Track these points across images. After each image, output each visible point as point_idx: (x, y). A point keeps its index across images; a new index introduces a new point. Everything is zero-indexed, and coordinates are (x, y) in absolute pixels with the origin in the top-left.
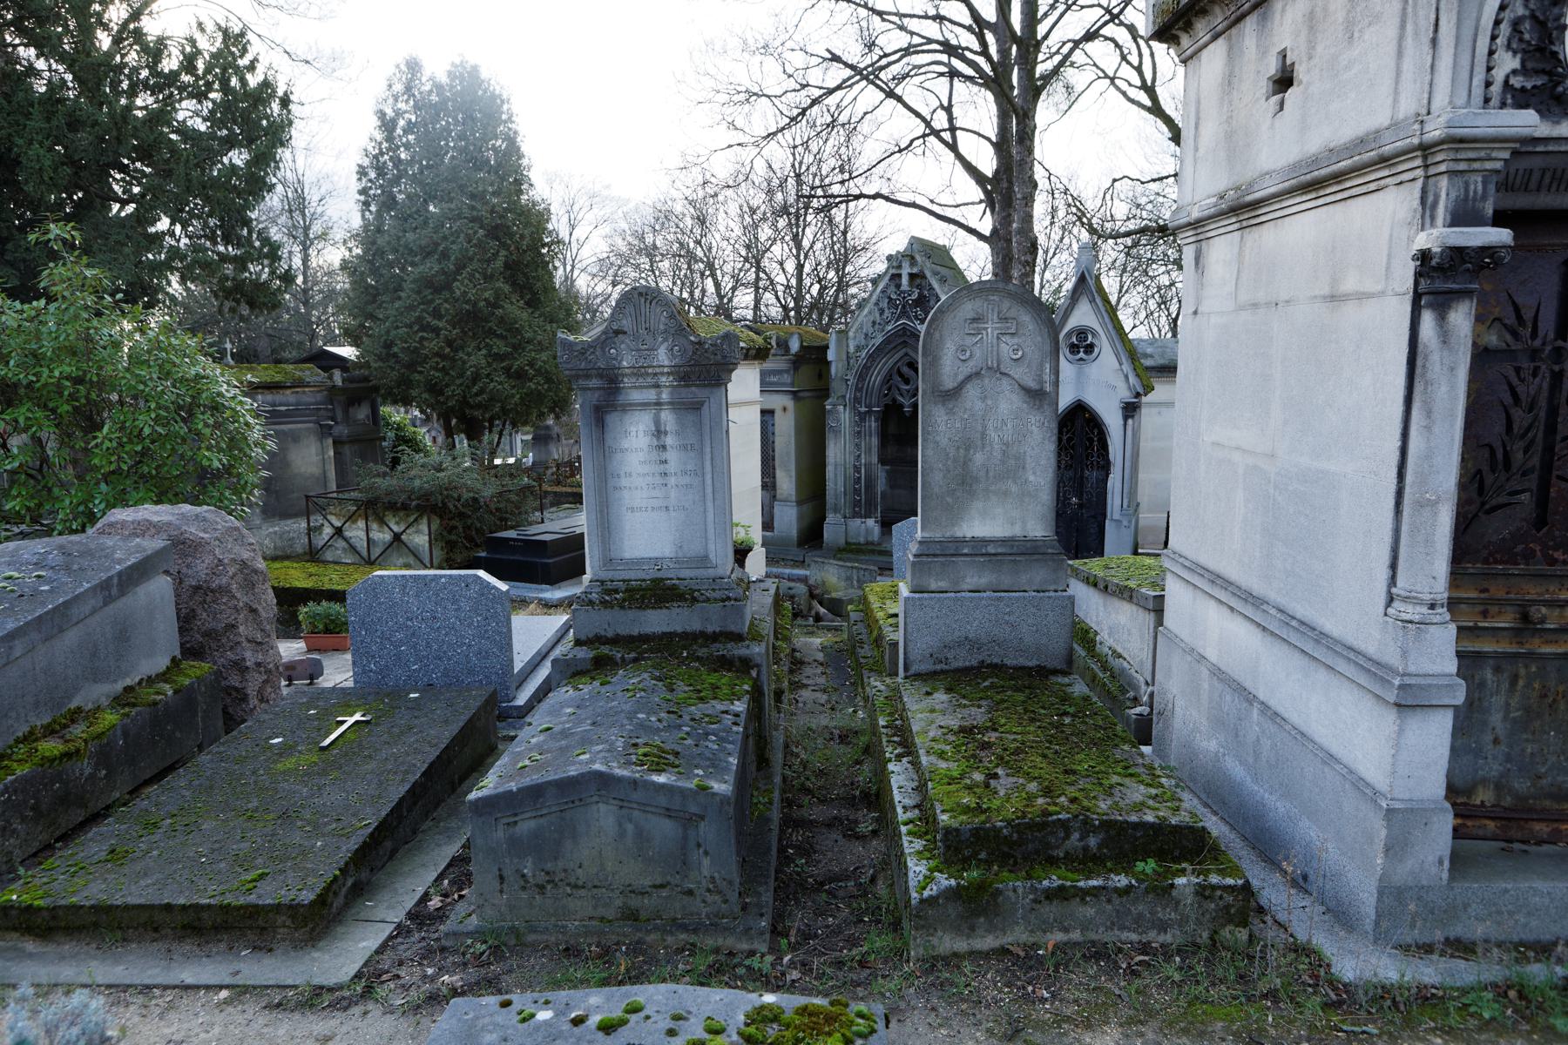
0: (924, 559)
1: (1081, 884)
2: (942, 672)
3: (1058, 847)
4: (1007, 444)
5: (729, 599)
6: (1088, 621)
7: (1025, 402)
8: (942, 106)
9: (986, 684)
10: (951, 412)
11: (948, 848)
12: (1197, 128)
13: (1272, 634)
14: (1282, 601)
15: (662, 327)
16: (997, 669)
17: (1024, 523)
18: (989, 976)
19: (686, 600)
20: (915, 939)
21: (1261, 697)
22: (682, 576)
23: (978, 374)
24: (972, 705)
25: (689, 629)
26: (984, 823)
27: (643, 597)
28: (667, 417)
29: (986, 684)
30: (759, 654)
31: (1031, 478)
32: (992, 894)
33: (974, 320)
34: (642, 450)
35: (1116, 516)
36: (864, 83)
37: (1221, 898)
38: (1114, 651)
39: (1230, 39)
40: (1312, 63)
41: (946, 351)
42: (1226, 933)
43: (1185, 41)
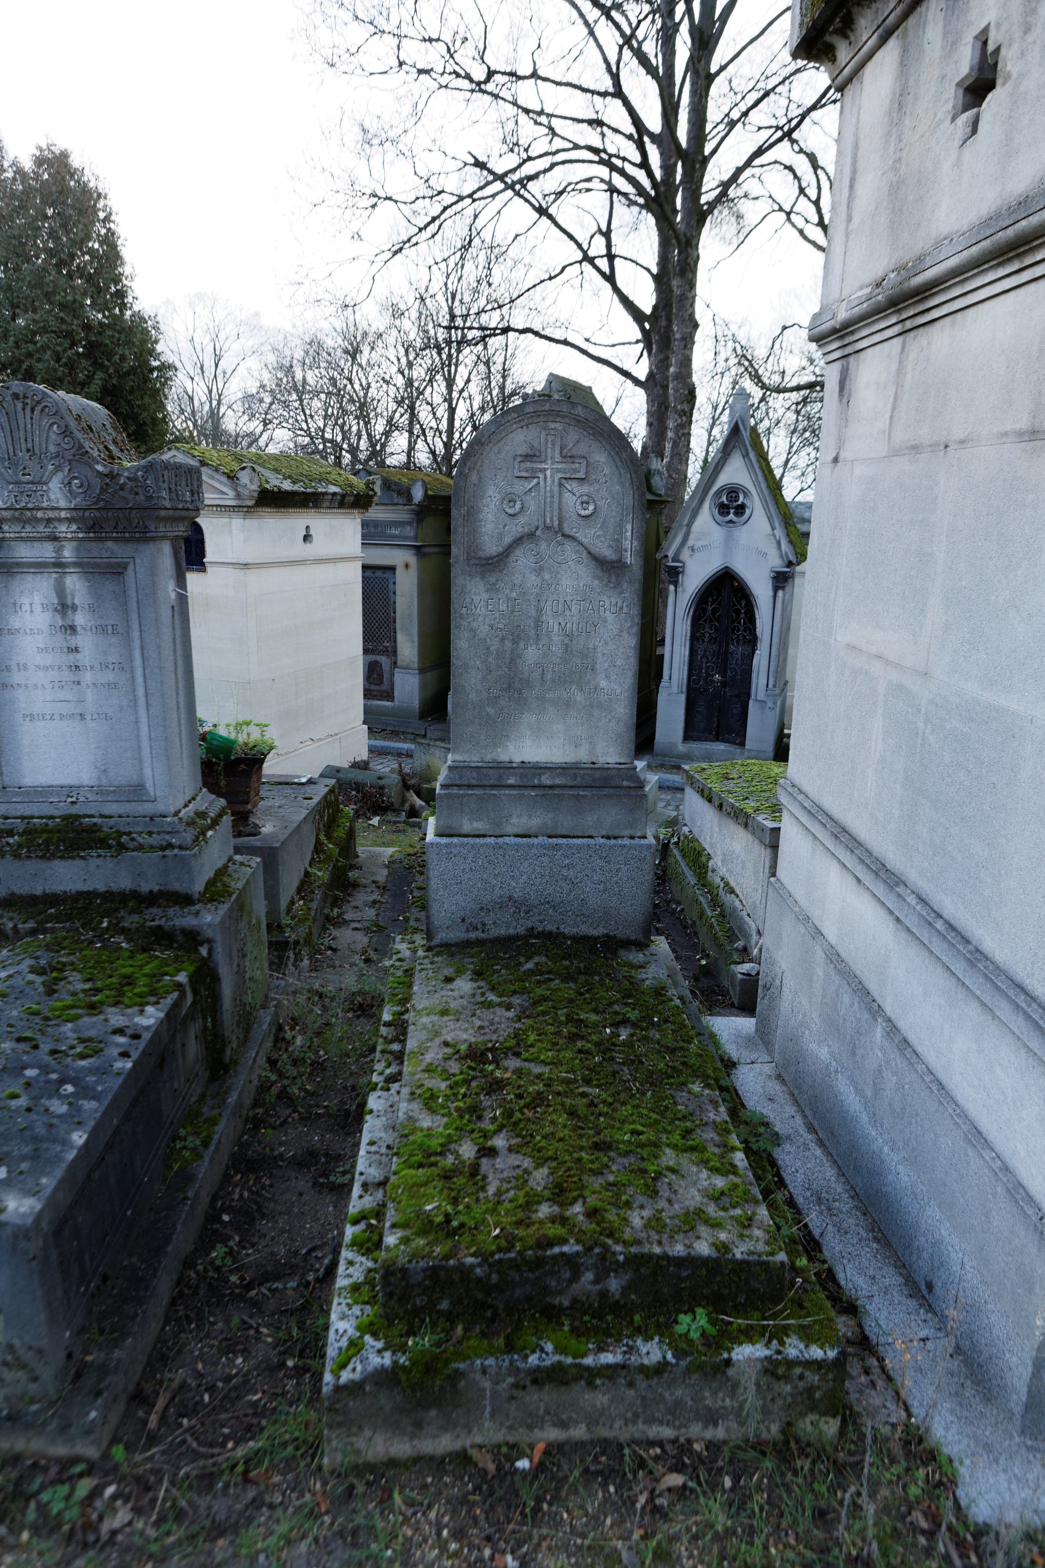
0: (455, 791)
1: (588, 1361)
2: (479, 942)
3: (561, 1293)
4: (570, 636)
5: (170, 846)
6: (701, 840)
7: (596, 577)
8: (600, 231)
9: (530, 965)
10: (492, 588)
11: (390, 1296)
12: (852, 187)
13: (908, 929)
14: (927, 888)
15: (52, 449)
16: (551, 939)
17: (592, 744)
18: (432, 1515)
19: (110, 847)
20: (329, 1441)
21: (888, 1009)
22: (106, 811)
23: (531, 536)
24: (500, 1005)
25: (114, 887)
26: (446, 1257)
27: (47, 842)
28: (75, 584)
29: (530, 965)
30: (210, 925)
31: (603, 684)
32: (449, 1377)
33: (527, 457)
34: (40, 632)
35: (761, 696)
36: (509, 193)
37: (801, 1377)
38: (727, 884)
39: (904, 36)
40: (1030, 38)
41: (486, 500)
42: (806, 1425)
43: (843, 53)
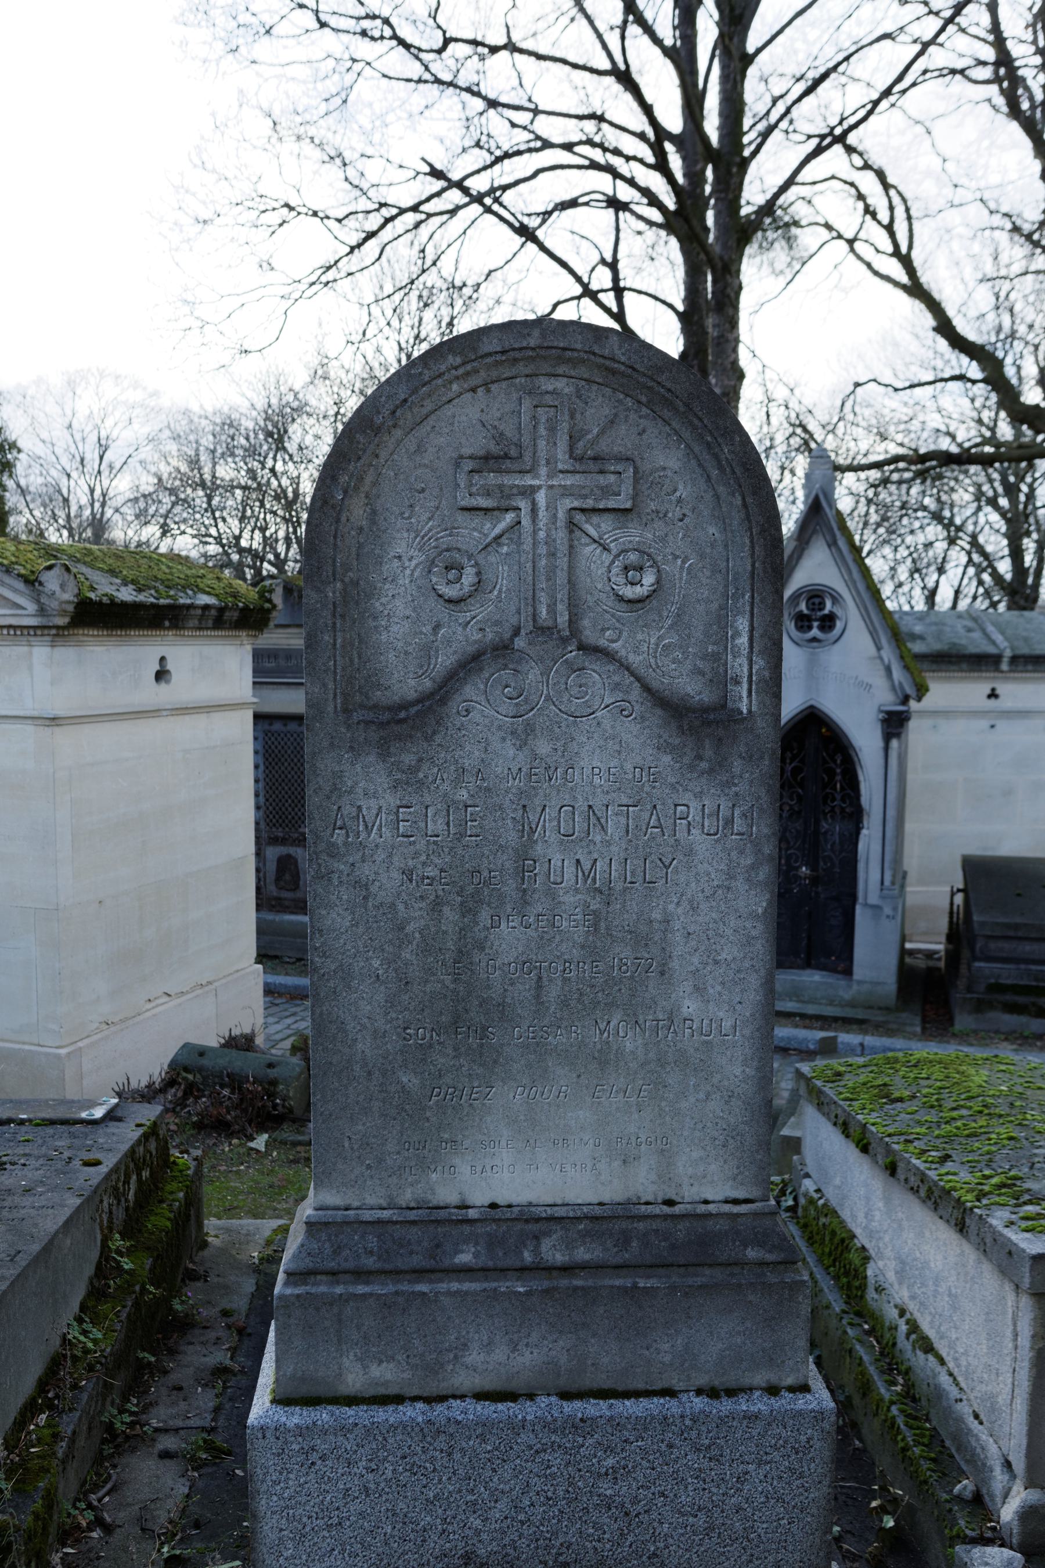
0: (322, 1288)
4: (605, 892)
6: (845, 1214)
8: (603, 261)
31: (690, 1007)
33: (488, 461)
35: (873, 899)
36: (476, 209)
38: (914, 1327)
